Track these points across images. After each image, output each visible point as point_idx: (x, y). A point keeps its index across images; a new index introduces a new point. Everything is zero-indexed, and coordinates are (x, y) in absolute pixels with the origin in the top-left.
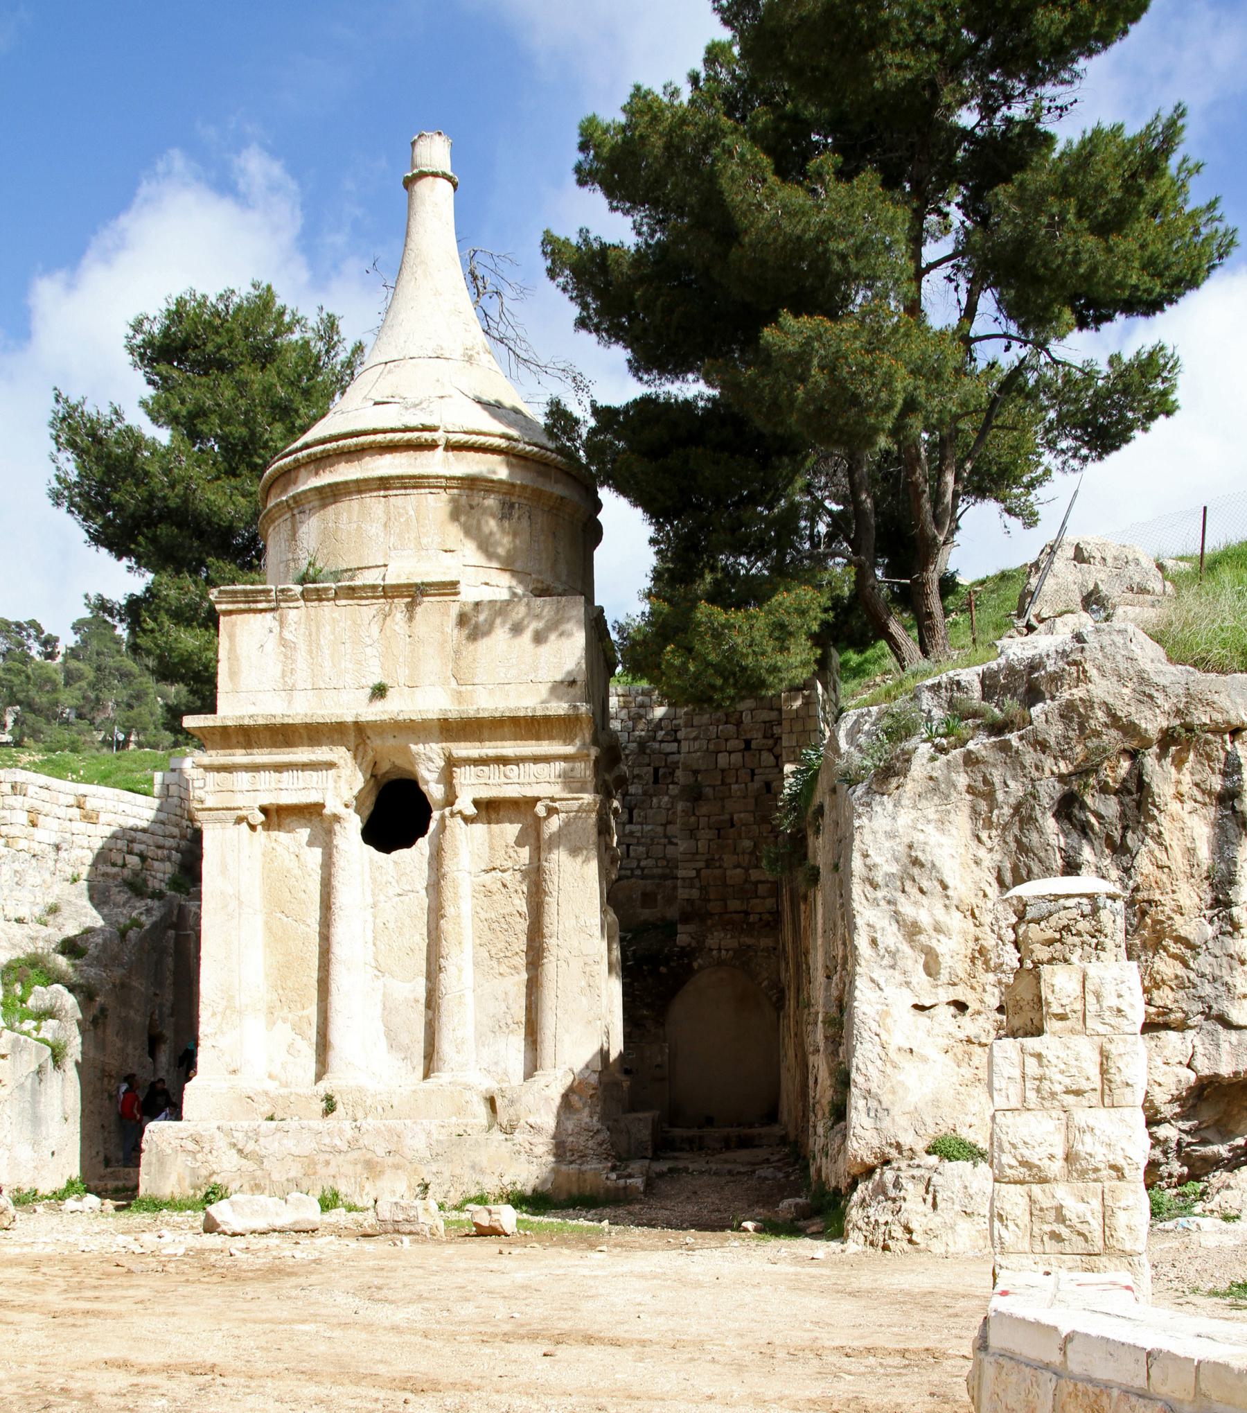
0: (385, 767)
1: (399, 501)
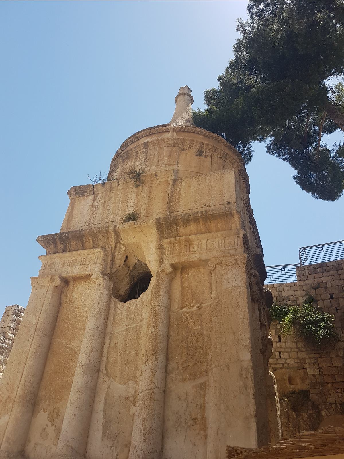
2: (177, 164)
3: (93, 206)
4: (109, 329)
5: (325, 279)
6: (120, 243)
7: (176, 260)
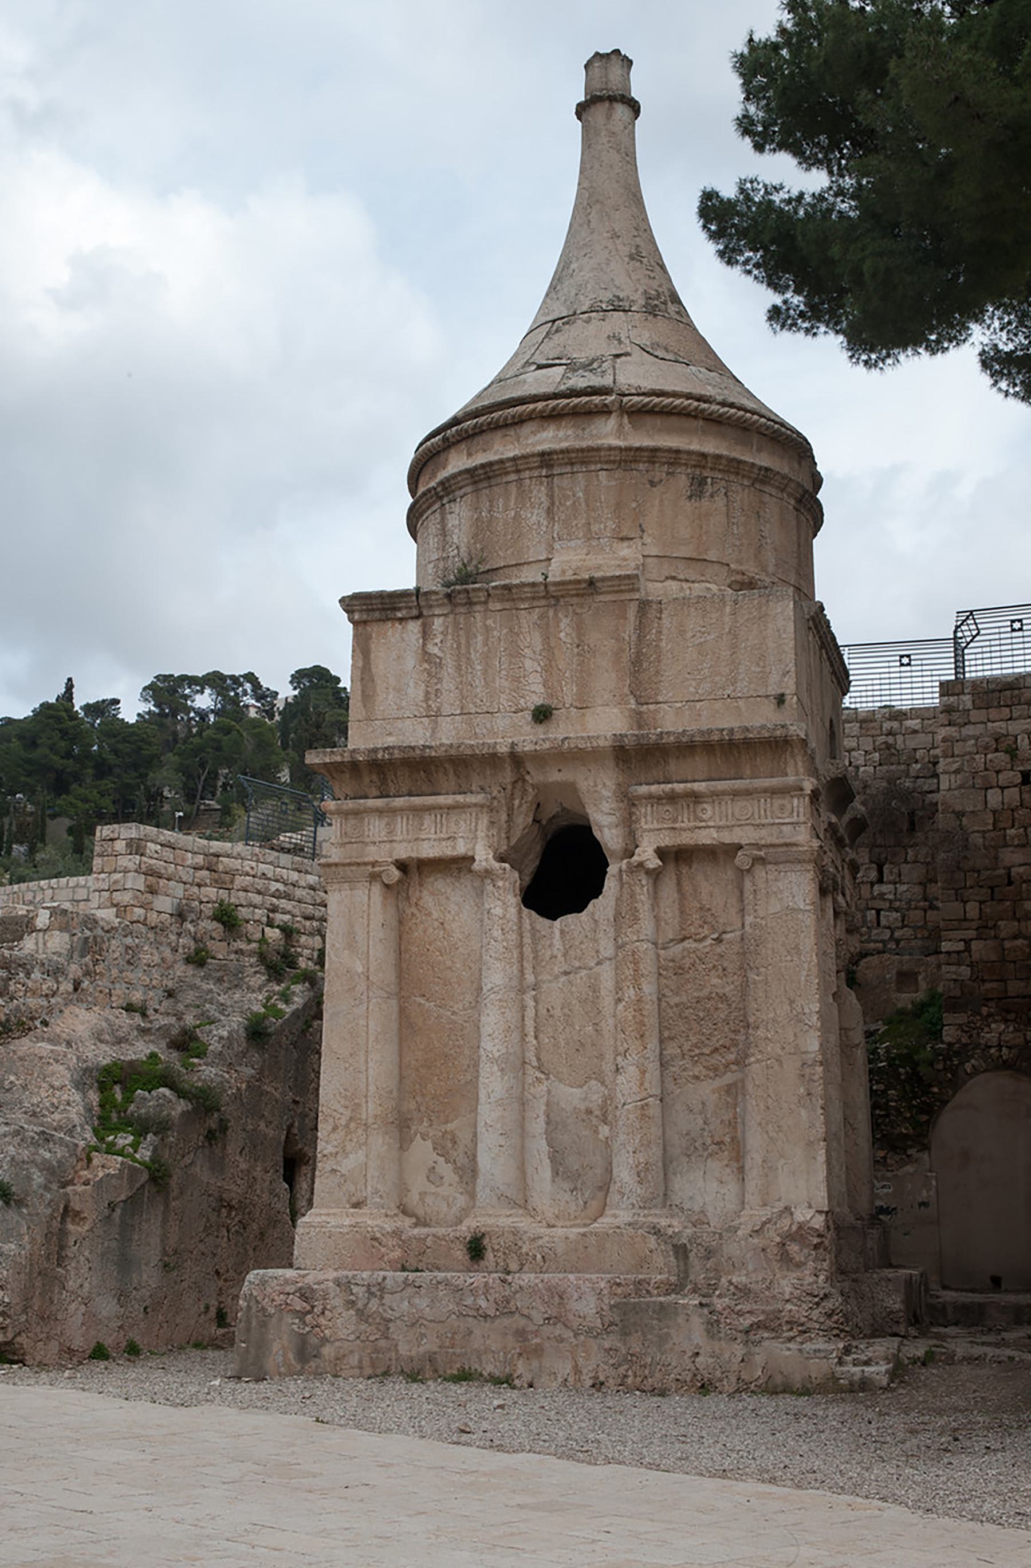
0: (551, 809)
1: (565, 482)
2: (641, 538)
3: (426, 656)
4: (530, 978)
5: (1014, 727)
6: (524, 781)
7: (666, 840)
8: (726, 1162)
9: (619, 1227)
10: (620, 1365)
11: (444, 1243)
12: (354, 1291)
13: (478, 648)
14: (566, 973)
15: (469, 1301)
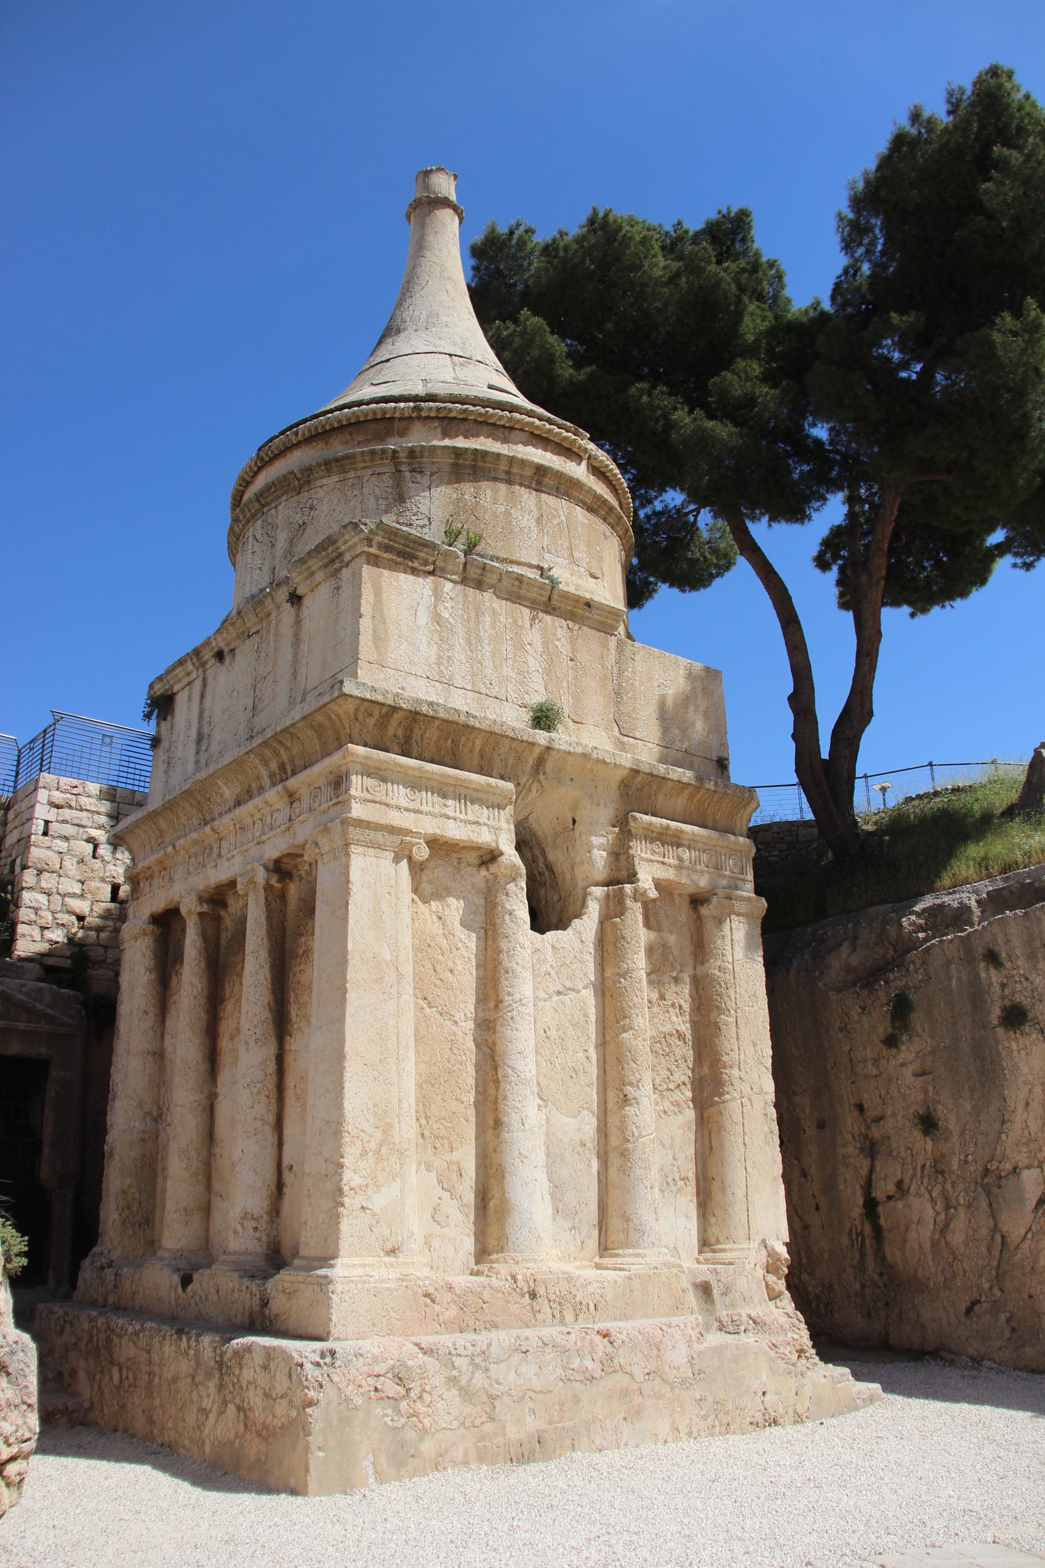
3: (437, 618)
8: (689, 1197)
9: (656, 1268)
10: (708, 1416)
11: (500, 1295)
12: (456, 1364)
13: (487, 627)
14: (559, 993)
15: (576, 1363)
